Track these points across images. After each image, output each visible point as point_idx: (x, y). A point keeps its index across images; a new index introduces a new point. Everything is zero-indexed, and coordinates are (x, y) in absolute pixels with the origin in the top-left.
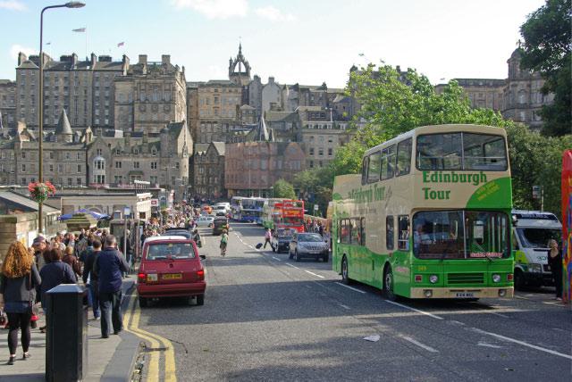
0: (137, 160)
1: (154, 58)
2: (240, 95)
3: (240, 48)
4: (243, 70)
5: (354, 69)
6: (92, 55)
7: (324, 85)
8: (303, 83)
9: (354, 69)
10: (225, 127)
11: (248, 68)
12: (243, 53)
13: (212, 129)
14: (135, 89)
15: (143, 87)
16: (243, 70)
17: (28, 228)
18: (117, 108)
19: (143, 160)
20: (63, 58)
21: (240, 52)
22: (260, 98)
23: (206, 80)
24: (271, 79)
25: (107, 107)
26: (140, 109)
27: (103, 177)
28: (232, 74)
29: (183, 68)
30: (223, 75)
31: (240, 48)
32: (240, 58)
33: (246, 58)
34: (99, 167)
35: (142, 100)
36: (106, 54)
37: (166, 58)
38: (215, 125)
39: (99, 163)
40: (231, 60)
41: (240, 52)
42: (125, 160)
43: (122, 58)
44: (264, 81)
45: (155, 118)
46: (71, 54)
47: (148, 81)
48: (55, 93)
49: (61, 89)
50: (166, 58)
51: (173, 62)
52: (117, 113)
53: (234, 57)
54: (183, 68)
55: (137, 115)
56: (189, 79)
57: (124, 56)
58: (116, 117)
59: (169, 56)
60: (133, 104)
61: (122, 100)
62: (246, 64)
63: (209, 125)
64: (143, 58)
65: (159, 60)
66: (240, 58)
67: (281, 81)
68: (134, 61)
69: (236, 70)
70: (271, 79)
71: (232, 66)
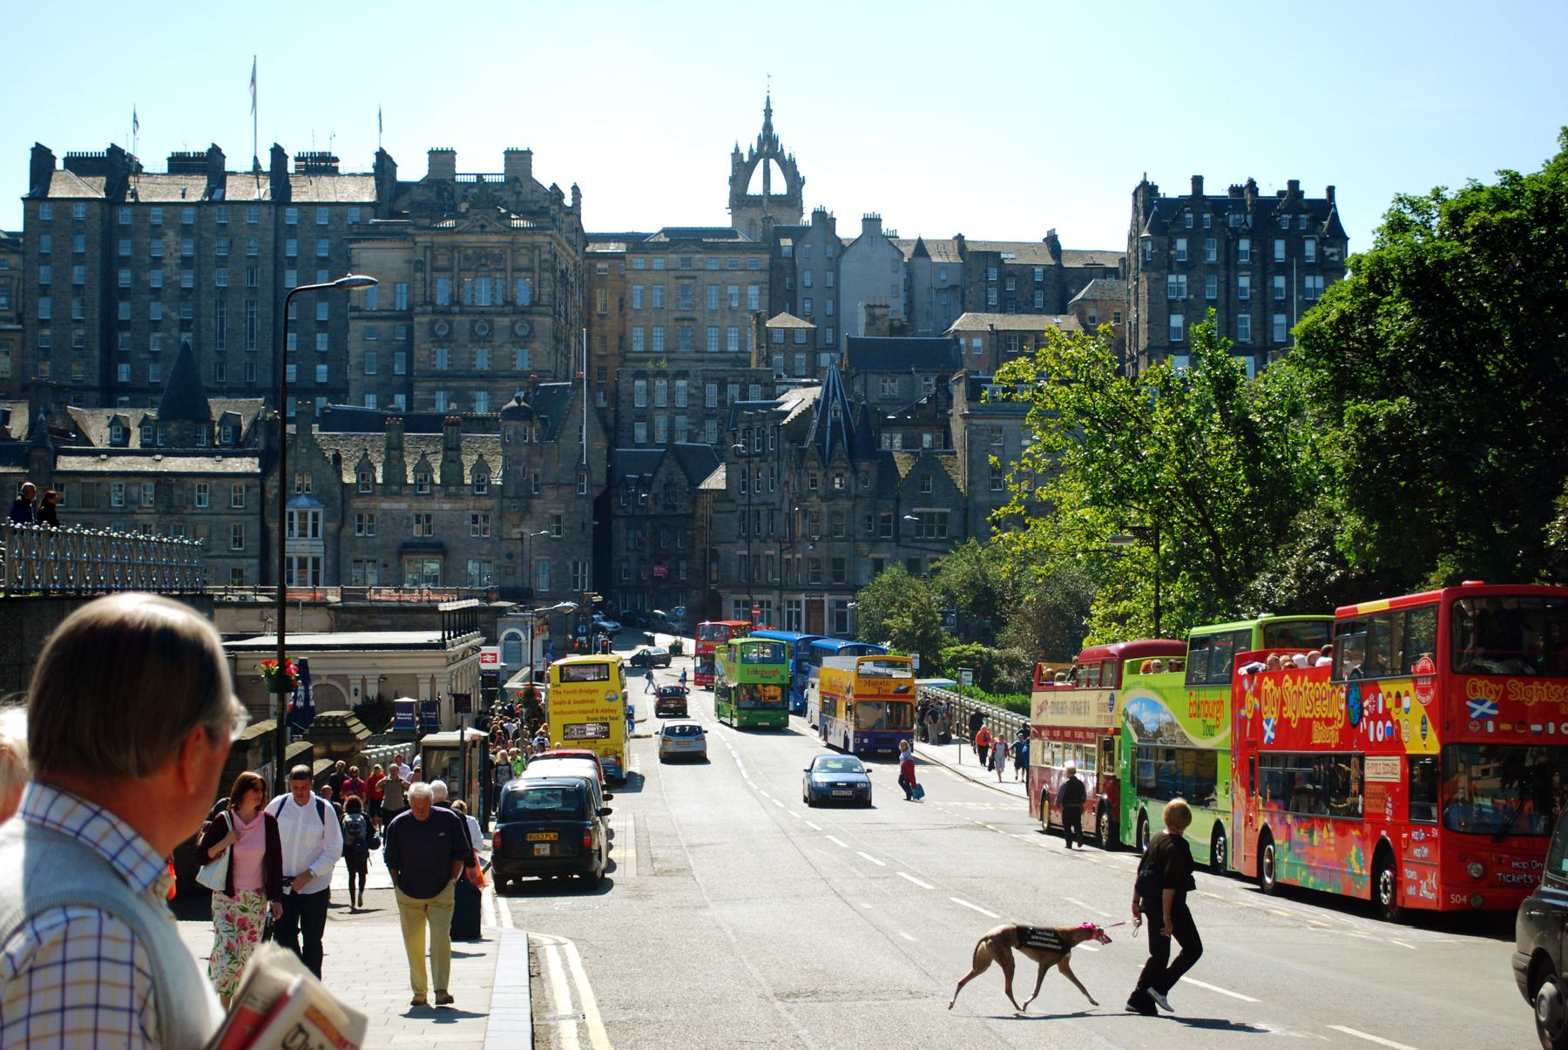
0: (424, 506)
1: (480, 161)
2: (764, 277)
3: (768, 112)
4: (779, 186)
5: (1146, 193)
6: (278, 154)
7: (1052, 241)
8: (980, 233)
9: (1146, 193)
10: (712, 389)
11: (795, 181)
12: (776, 131)
13: (671, 396)
14: (419, 266)
15: (442, 262)
16: (779, 186)
17: (260, 759)
18: (356, 328)
19: (446, 506)
20: (180, 164)
21: (768, 127)
22: (835, 292)
23: (650, 223)
24: (871, 223)
25: (322, 326)
26: (432, 333)
27: (316, 561)
28: (739, 200)
29: (575, 189)
30: (717, 215)
31: (768, 112)
32: (769, 145)
33: (788, 143)
34: (303, 535)
35: (442, 300)
36: (319, 148)
37: (518, 160)
38: (681, 383)
39: (303, 516)
40: (737, 155)
41: (768, 127)
42: (385, 505)
43: (373, 159)
44: (849, 229)
45: (482, 362)
46: (204, 148)
47: (459, 238)
48: (156, 279)
49: (172, 262)
50: (518, 160)
51: (544, 174)
52: (355, 347)
53: (748, 141)
54: (575, 189)
55: (422, 351)
56: (590, 225)
57: (382, 156)
58: (353, 361)
59: (529, 153)
60: (407, 316)
61: (373, 304)
62: (789, 168)
63: (661, 384)
64: (442, 159)
65: (494, 168)
66: (769, 145)
67: (906, 225)
68: (412, 170)
69: (755, 187)
70: (871, 223)
71: (741, 170)
